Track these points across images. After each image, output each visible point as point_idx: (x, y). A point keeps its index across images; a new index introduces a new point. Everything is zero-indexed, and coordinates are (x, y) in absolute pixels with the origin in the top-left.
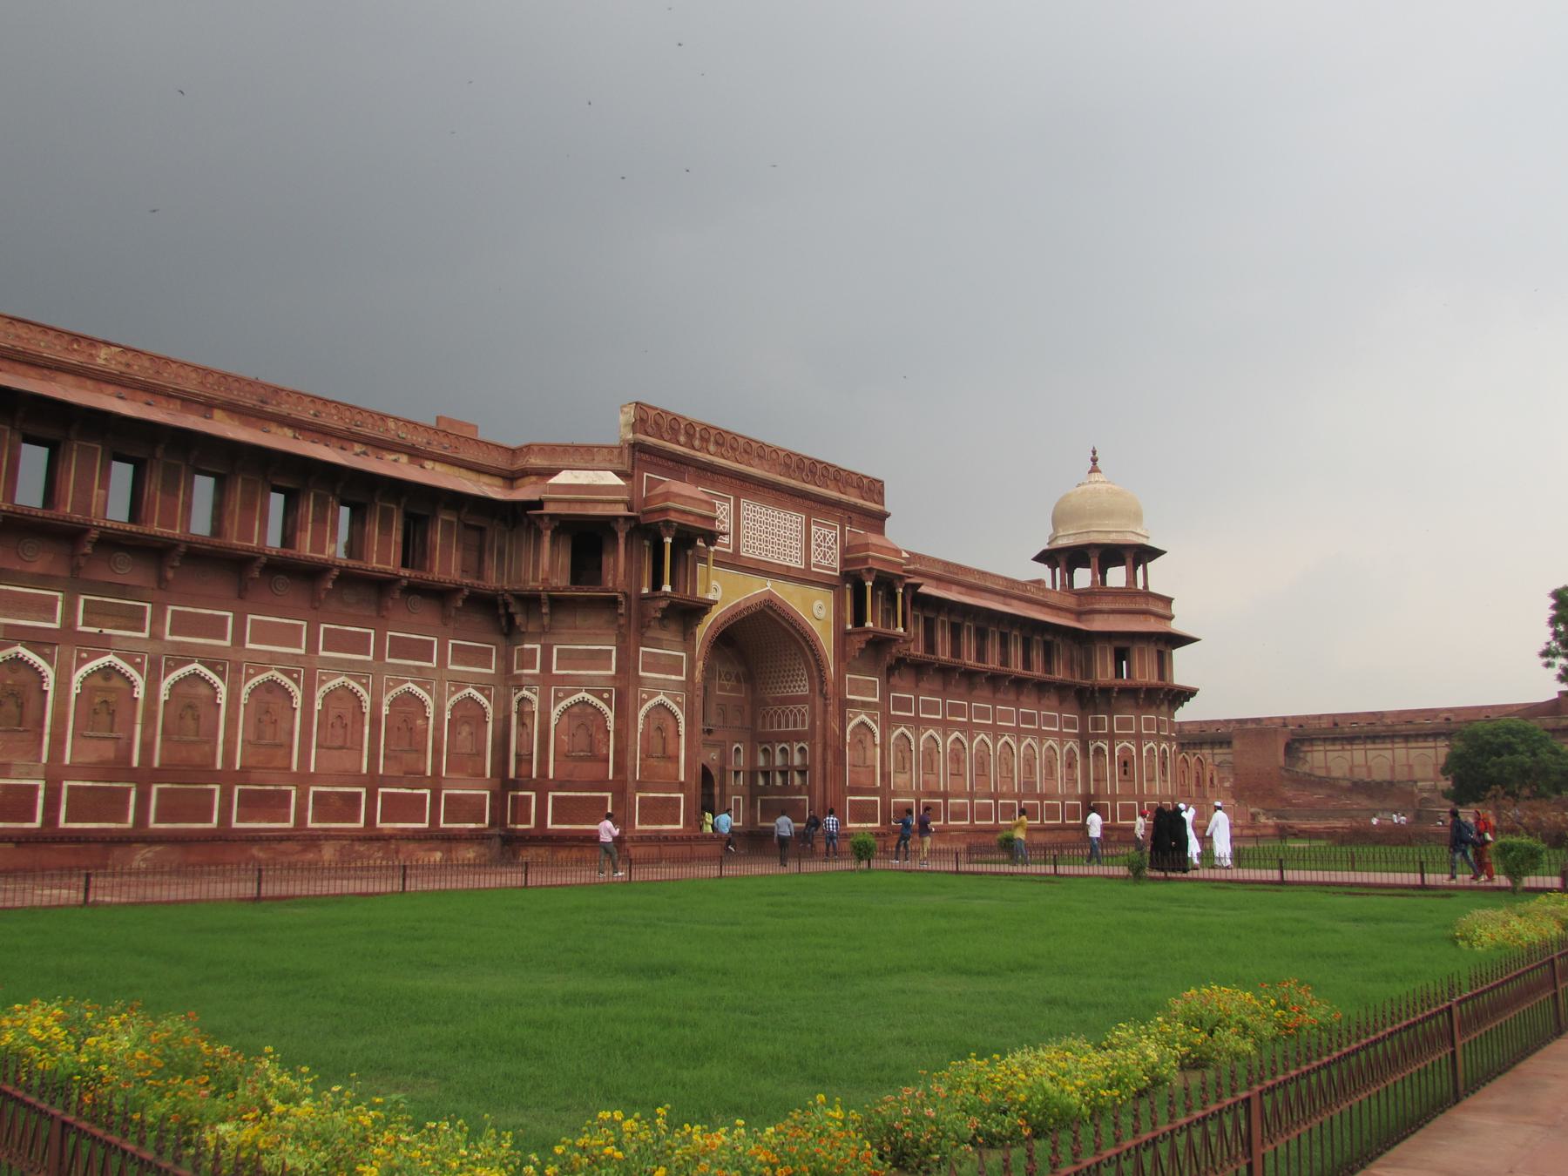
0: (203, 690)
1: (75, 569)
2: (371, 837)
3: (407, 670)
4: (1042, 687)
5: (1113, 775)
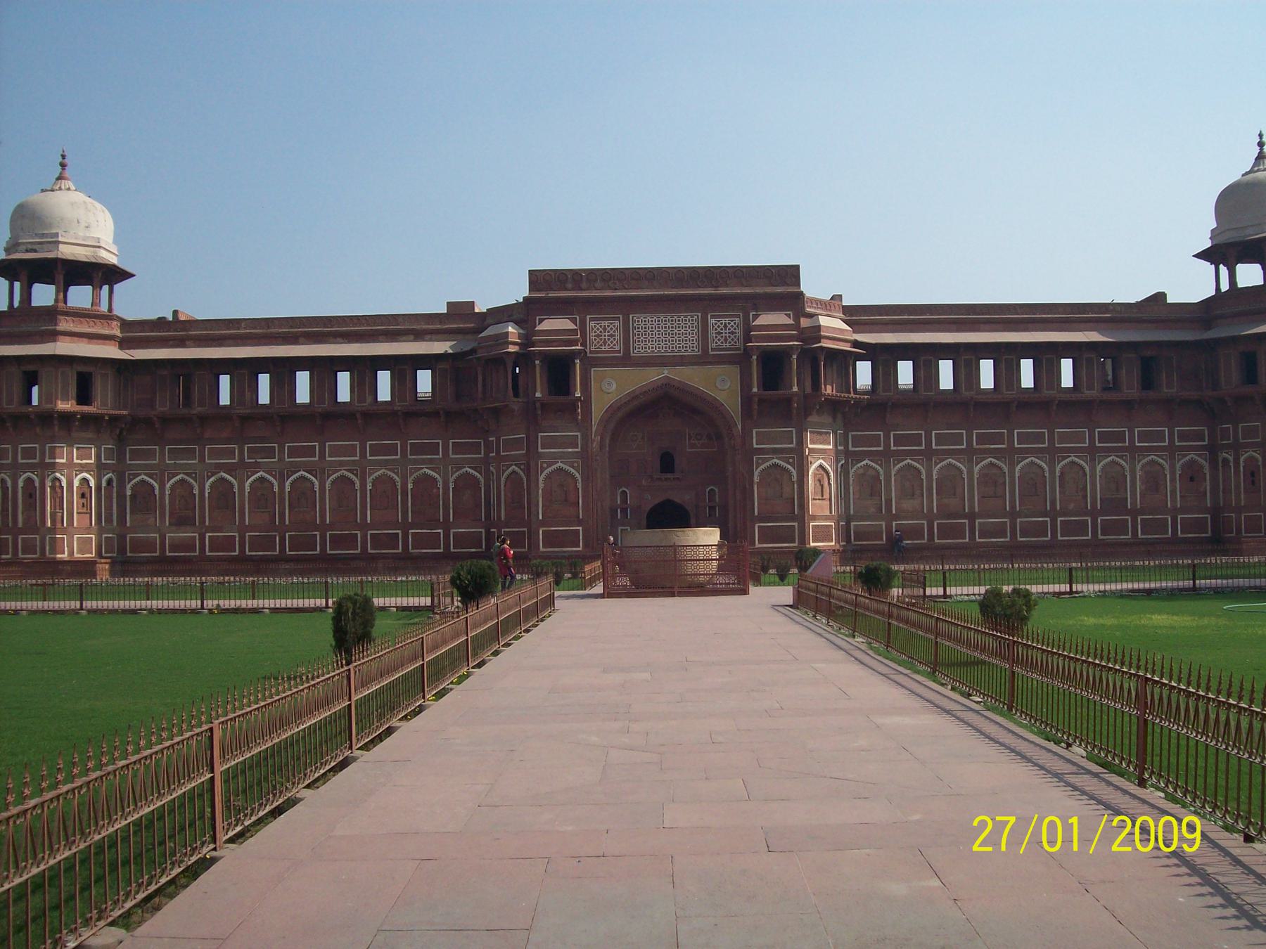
0: (309, 485)
3: (423, 462)
5: (1237, 487)
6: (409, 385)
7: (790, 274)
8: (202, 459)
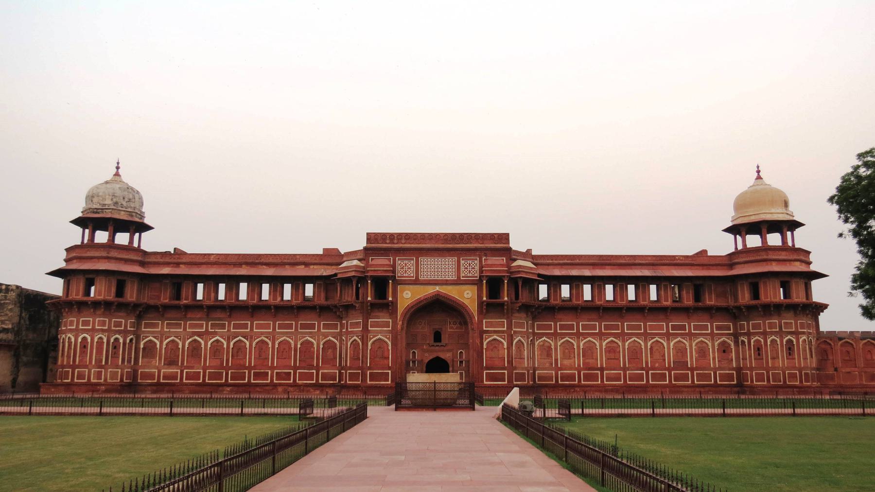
1: (208, 315)
2: (295, 385)
4: (686, 311)
5: (750, 356)
6: (301, 291)
7: (505, 237)
8: (185, 329)
